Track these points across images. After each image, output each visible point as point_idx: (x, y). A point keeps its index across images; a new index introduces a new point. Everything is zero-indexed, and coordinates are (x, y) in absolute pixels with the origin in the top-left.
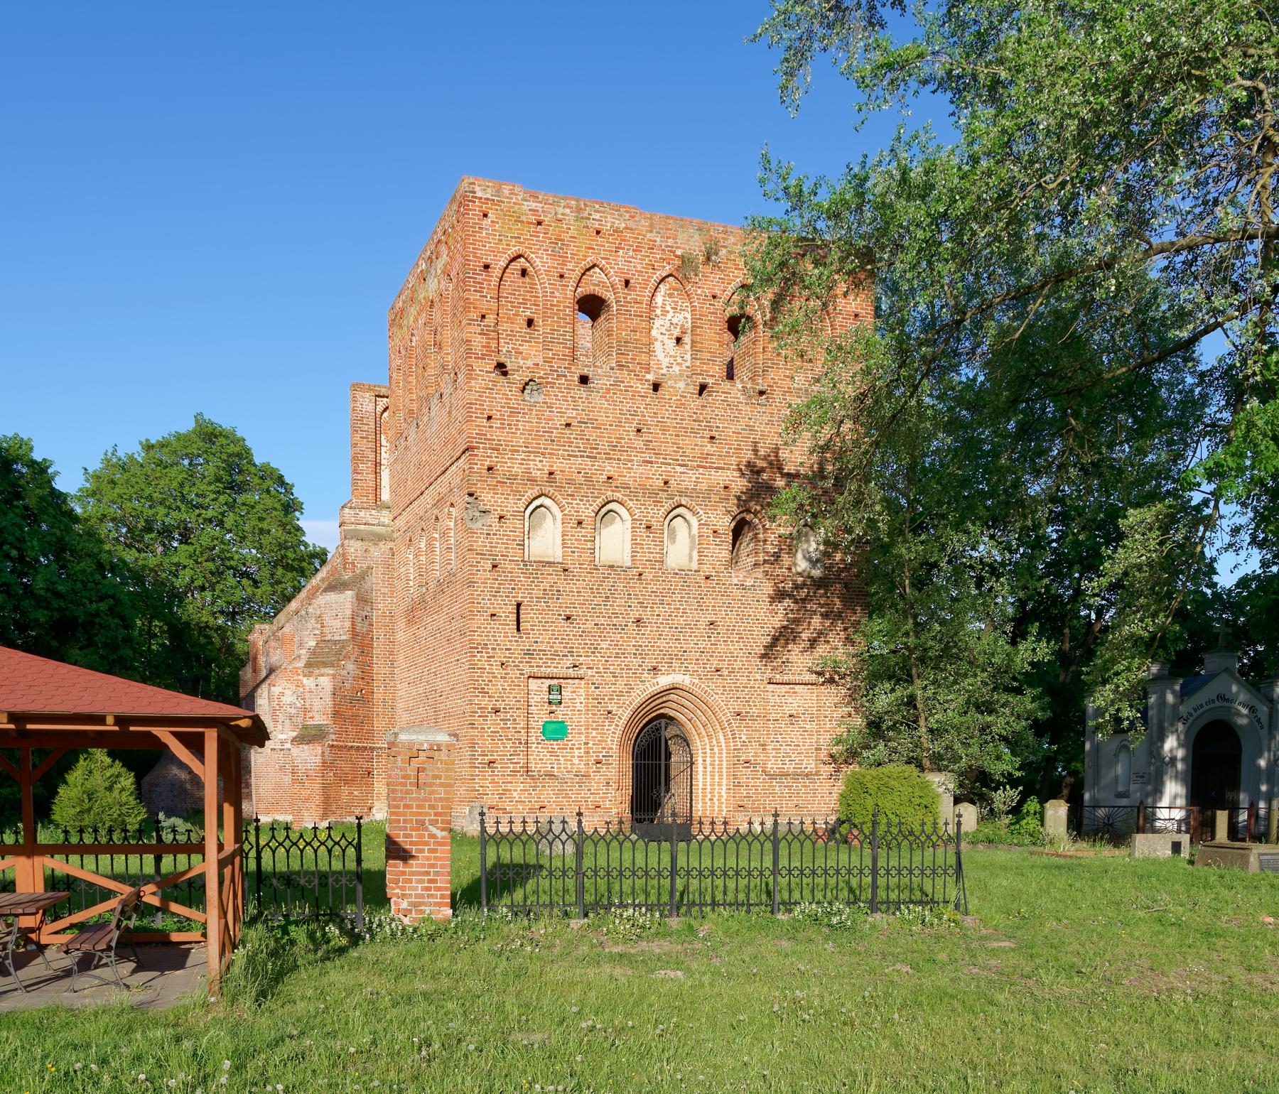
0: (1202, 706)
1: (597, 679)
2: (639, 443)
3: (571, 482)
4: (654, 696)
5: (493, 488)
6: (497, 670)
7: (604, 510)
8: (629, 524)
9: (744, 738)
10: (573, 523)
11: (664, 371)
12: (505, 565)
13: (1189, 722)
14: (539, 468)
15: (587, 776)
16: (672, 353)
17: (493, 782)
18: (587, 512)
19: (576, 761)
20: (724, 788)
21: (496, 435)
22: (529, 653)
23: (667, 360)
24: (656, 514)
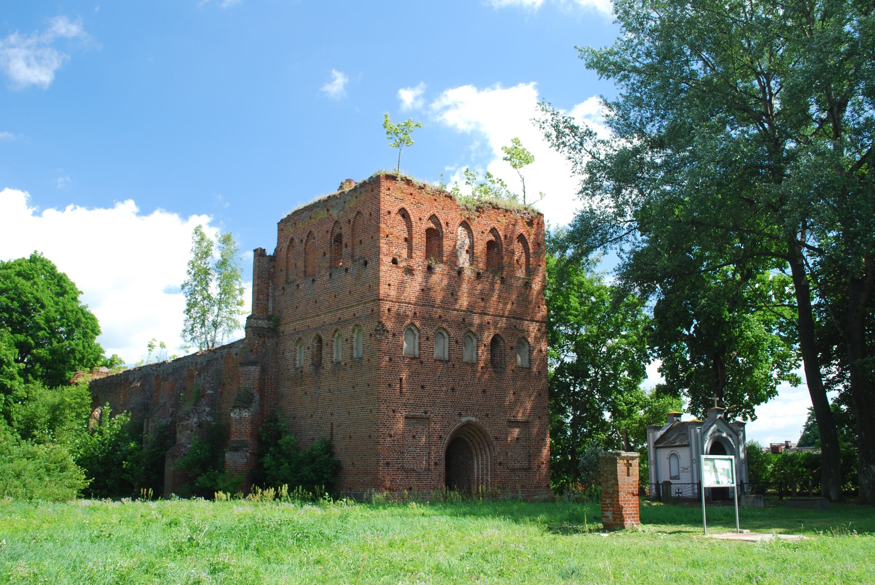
1: (435, 419)
6: (391, 414)
8: (447, 340)
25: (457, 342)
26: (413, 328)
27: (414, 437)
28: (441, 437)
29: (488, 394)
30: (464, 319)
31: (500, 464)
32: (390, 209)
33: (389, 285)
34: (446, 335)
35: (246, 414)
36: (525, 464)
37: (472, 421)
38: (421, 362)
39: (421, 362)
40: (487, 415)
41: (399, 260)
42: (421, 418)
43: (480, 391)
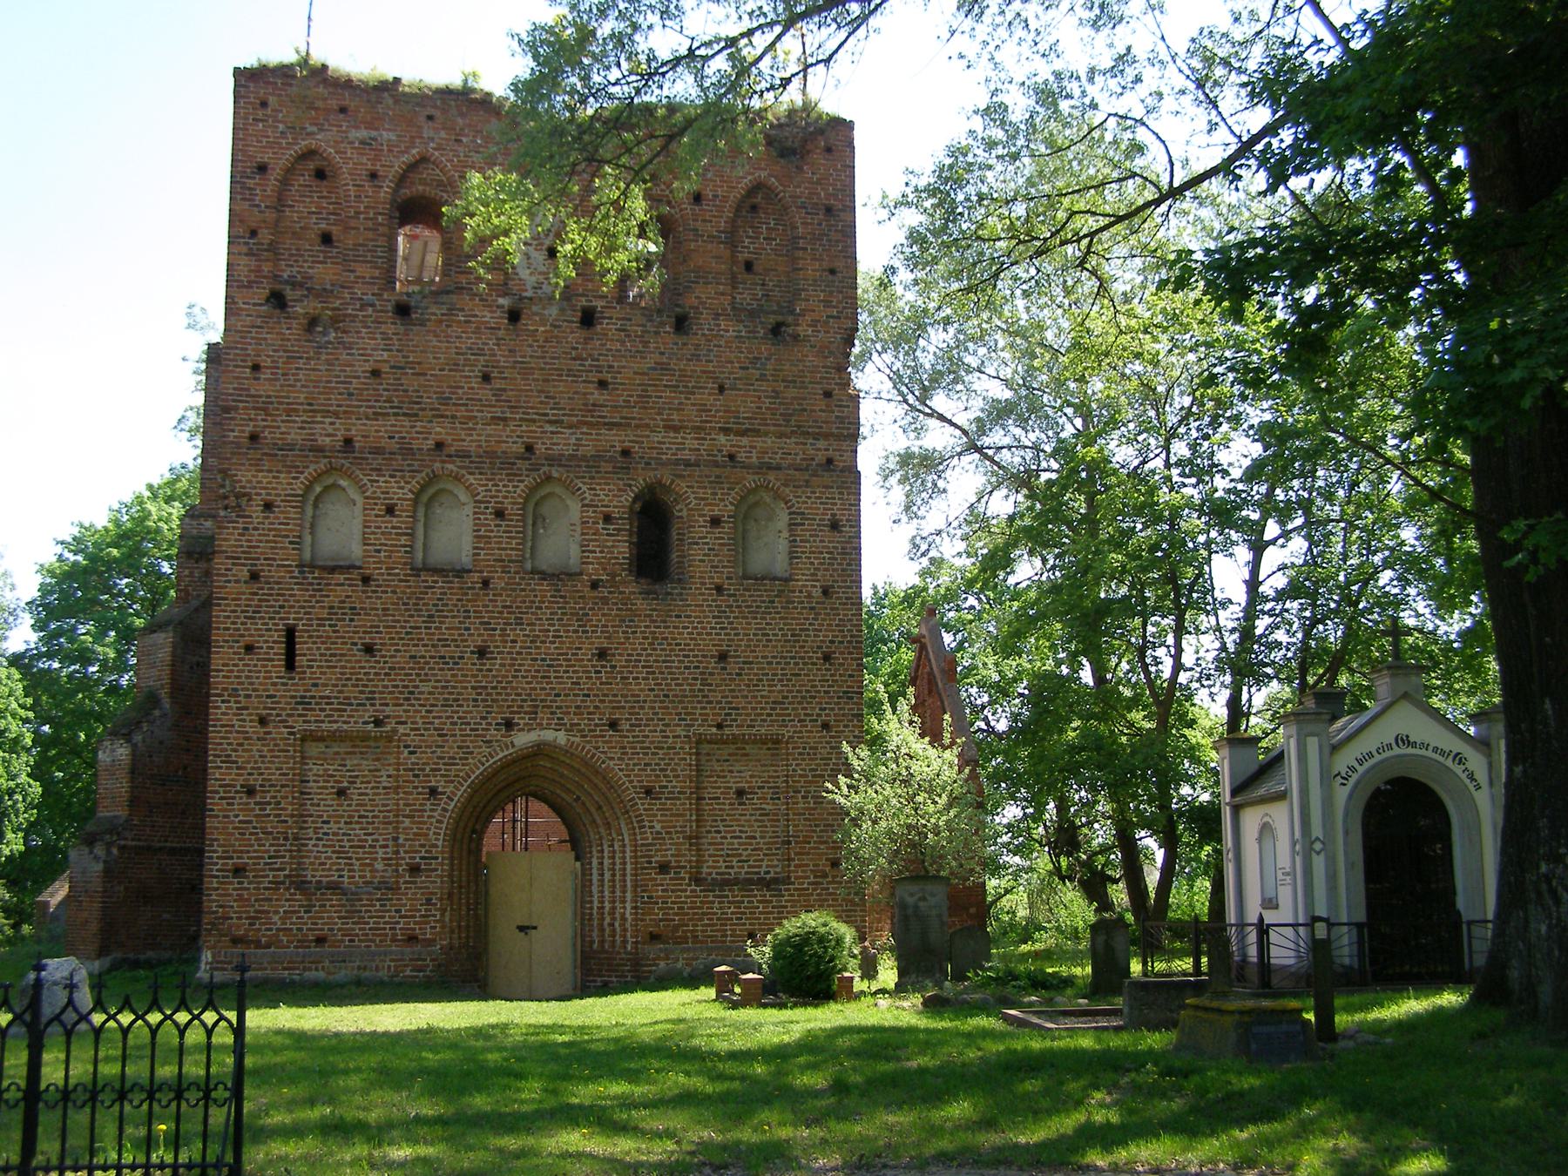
0: (1370, 755)
1: (413, 739)
2: (485, 393)
3: (378, 451)
4: (507, 764)
5: (257, 464)
6: (253, 728)
7: (431, 491)
8: (469, 510)
9: (658, 827)
10: (380, 509)
11: (529, 294)
12: (271, 573)
13: (1352, 781)
14: (328, 433)
15: (395, 889)
16: (544, 269)
17: (240, 898)
18: (401, 492)
19: (379, 866)
20: (628, 905)
21: (263, 387)
22: (303, 702)
23: (533, 279)
24: (511, 492)
25: (500, 514)
26: (343, 483)
27: (341, 793)
28: (433, 792)
29: (619, 661)
30: (529, 448)
31: (664, 868)
32: (266, 158)
33: (256, 368)
34: (463, 496)
35: (123, 752)
36: (770, 867)
37: (553, 746)
38: (366, 580)
39: (366, 580)
40: (613, 725)
41: (289, 293)
42: (365, 737)
43: (587, 651)
